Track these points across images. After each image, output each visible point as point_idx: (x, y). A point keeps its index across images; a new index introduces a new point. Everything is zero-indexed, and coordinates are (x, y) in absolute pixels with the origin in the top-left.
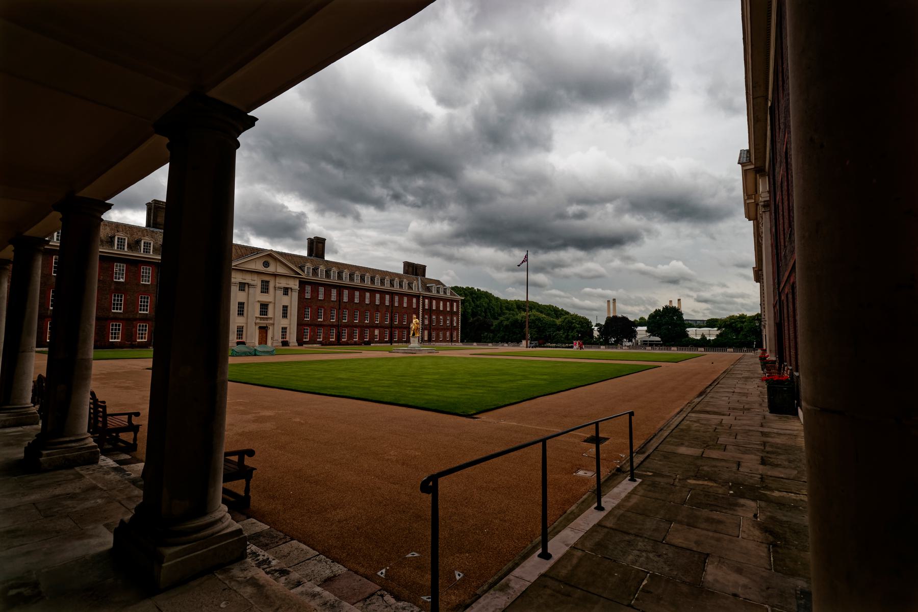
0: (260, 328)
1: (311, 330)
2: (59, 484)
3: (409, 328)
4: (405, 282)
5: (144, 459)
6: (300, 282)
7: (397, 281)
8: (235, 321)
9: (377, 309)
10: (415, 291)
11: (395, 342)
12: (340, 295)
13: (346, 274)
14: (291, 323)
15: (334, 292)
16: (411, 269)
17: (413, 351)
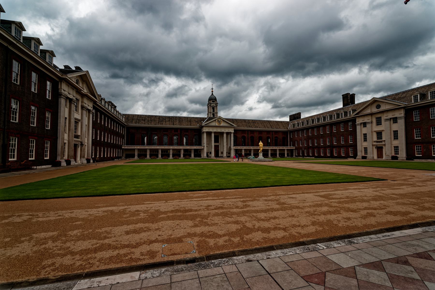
8: (361, 145)
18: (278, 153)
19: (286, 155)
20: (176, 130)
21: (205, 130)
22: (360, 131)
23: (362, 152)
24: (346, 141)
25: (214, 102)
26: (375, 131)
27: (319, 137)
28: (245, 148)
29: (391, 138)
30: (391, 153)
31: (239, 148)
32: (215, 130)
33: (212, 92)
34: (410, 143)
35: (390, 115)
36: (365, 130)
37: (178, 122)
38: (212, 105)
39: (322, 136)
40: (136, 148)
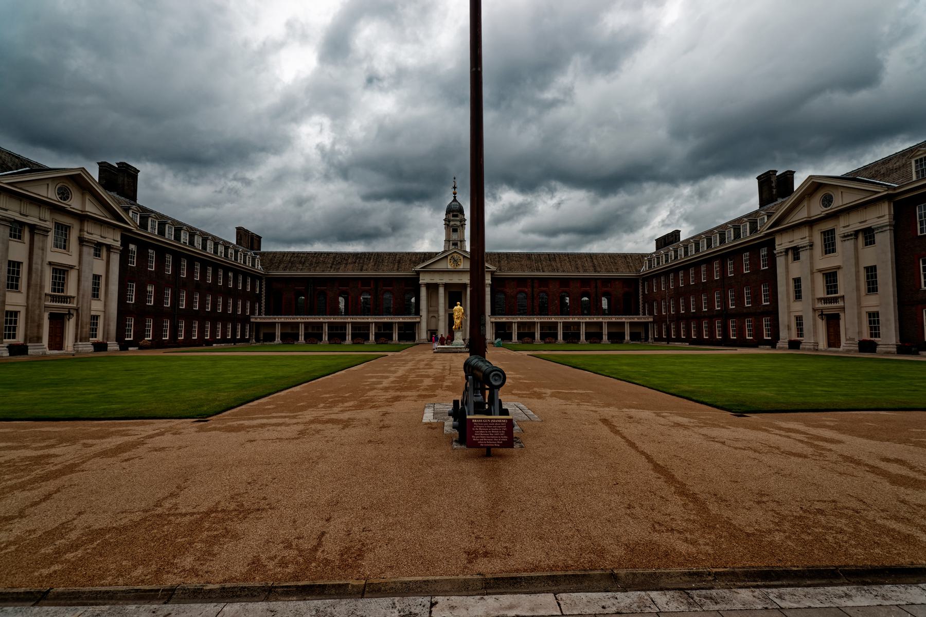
18: (605, 331)
19: (627, 338)
20: (365, 281)
21: (424, 279)
22: (787, 271)
23: (789, 328)
24: (756, 299)
25: (456, 216)
26: (820, 271)
27: (700, 289)
28: (519, 319)
29: (858, 289)
30: (860, 333)
31: (504, 319)
32: (446, 279)
33: (455, 194)
35: (854, 222)
36: (797, 269)
37: (372, 263)
38: (452, 223)
40: (277, 320)
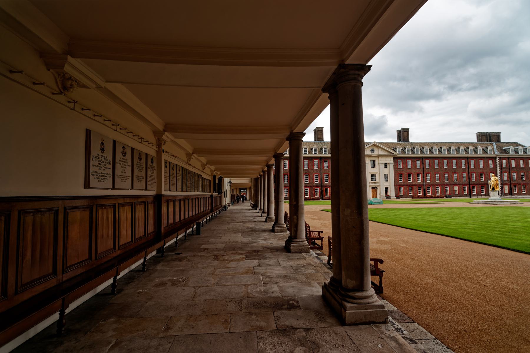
0: (372, 188)
1: (403, 188)
2: (298, 259)
3: (487, 185)
4: (480, 148)
5: (327, 254)
6: (394, 158)
7: (471, 149)
9: (455, 172)
10: (490, 154)
11: (474, 195)
12: (423, 164)
13: (426, 149)
14: (391, 184)
15: (418, 163)
16: (484, 138)
17: (493, 203)
34: (397, 186)
35: (384, 160)
39: (455, 172)
